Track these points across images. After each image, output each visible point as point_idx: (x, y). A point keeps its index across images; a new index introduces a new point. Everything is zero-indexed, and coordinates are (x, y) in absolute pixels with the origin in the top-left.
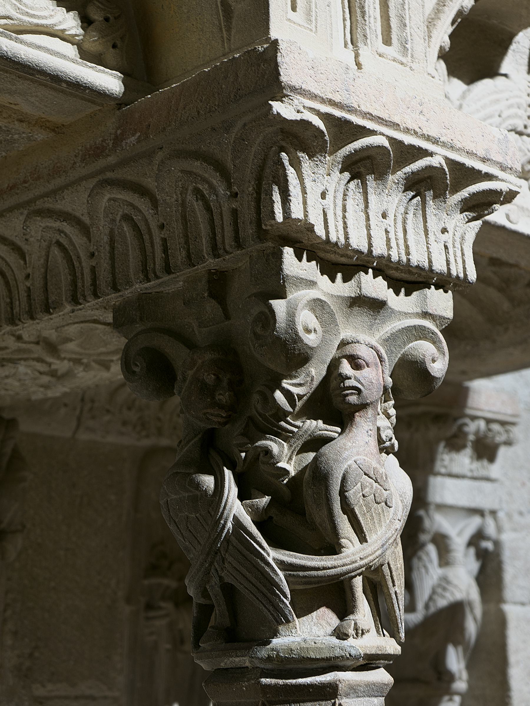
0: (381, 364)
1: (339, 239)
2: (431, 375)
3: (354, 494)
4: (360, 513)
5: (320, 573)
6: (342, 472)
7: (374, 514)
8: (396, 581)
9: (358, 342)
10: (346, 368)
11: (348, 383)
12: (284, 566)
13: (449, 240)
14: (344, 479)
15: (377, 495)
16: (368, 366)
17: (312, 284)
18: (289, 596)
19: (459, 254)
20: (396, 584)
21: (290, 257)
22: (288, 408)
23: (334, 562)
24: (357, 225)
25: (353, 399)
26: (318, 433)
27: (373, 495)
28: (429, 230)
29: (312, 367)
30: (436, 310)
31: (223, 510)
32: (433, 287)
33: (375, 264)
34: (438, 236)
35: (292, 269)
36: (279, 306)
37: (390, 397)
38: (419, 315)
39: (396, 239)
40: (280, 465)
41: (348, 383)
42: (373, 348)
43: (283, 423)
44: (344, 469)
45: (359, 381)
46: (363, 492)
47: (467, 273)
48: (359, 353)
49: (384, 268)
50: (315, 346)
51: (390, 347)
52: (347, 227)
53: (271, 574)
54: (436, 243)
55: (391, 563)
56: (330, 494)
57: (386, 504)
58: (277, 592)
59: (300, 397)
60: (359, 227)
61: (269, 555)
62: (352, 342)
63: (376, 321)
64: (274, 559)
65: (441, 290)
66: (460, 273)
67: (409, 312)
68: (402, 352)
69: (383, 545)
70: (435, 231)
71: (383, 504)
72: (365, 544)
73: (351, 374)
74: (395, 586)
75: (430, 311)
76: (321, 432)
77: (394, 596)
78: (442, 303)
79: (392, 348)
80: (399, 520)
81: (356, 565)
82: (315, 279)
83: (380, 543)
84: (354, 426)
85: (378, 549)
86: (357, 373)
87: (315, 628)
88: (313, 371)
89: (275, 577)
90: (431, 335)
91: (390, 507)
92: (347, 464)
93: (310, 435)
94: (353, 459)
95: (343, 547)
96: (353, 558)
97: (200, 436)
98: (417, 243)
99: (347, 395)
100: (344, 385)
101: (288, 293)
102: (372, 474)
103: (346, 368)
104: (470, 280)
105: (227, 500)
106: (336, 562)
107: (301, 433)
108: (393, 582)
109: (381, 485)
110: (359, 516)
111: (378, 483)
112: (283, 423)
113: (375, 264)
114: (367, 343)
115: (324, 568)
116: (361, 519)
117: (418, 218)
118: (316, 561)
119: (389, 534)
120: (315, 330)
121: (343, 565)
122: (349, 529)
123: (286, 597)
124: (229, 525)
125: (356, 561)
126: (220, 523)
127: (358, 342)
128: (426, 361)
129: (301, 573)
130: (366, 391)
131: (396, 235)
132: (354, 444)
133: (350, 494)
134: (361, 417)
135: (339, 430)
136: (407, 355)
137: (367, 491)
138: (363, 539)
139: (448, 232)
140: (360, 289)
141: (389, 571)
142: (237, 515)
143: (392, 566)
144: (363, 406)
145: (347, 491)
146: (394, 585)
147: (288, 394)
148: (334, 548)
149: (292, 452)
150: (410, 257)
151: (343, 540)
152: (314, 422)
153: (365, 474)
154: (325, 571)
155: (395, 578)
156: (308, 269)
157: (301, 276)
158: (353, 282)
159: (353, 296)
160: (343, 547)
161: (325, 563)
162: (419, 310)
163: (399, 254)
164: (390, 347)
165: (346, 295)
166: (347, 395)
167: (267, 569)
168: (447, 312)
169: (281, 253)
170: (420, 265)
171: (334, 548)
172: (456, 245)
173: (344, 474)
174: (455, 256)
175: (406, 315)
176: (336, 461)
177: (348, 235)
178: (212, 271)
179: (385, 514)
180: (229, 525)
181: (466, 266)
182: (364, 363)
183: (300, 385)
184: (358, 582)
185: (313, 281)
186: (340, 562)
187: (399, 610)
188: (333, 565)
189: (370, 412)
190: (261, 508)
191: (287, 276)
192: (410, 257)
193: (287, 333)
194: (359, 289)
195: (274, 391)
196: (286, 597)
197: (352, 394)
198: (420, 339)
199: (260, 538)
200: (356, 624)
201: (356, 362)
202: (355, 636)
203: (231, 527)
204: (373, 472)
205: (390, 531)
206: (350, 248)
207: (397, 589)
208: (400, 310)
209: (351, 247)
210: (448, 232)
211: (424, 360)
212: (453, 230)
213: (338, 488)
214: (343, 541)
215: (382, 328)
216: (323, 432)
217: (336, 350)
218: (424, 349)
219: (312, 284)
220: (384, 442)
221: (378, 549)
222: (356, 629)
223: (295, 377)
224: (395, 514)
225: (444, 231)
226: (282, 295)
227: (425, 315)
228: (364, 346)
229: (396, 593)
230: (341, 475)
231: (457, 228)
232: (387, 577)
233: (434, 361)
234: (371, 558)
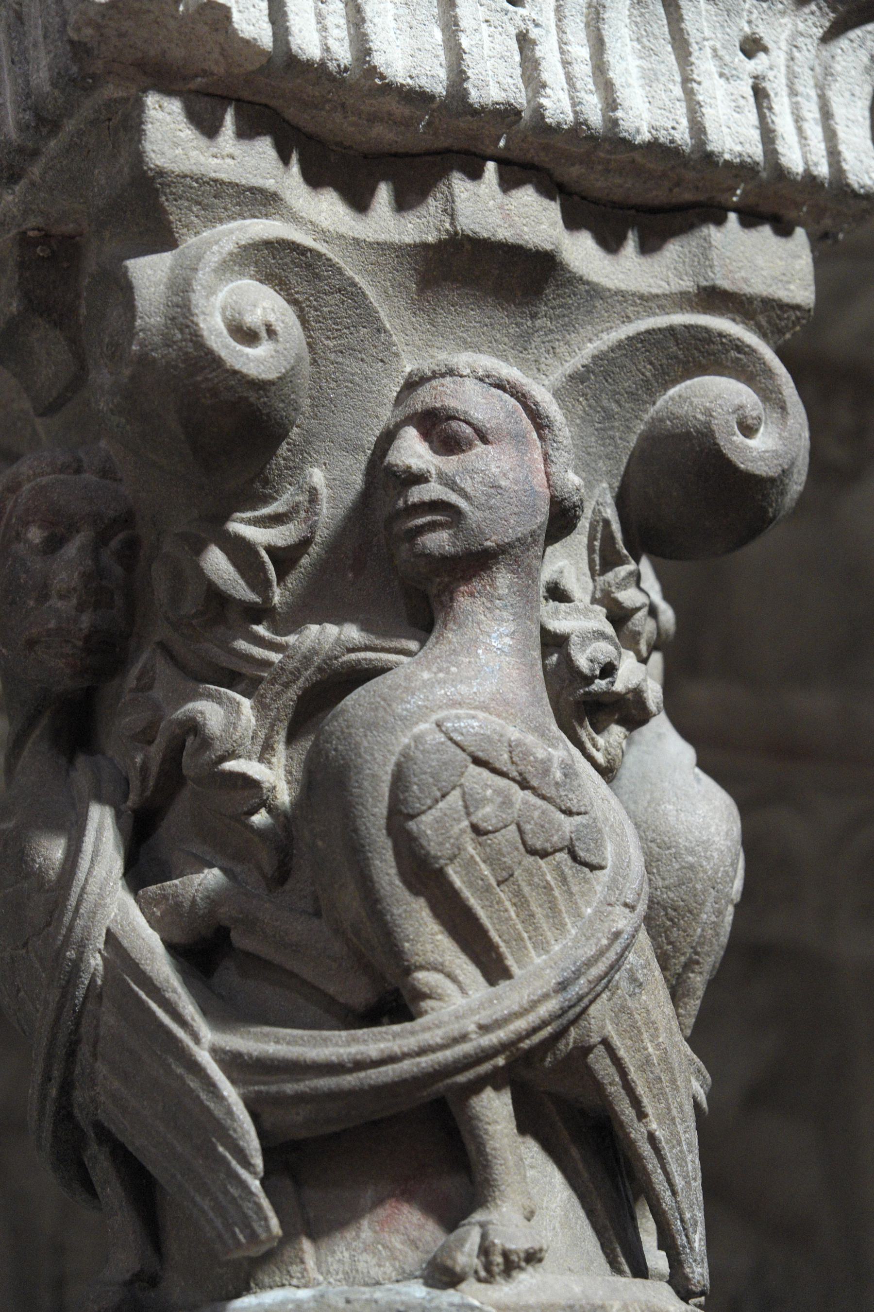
0: (541, 437)
1: (327, 50)
2: (736, 469)
3: (439, 826)
4: (471, 885)
5: (349, 1081)
6: (393, 759)
7: (526, 890)
8: (645, 1101)
9: (451, 372)
10: (413, 451)
11: (418, 494)
12: (236, 1065)
13: (770, 75)
14: (400, 779)
15: (527, 827)
16: (485, 440)
17: (263, 201)
18: (258, 1161)
19: (811, 111)
20: (649, 1110)
21: (168, 118)
22: (241, 590)
23: (389, 1044)
24: (409, 18)
25: (439, 541)
26: (345, 658)
27: (513, 827)
28: (692, 40)
29: (315, 463)
30: (746, 280)
31: (74, 919)
32: (732, 216)
33: (502, 144)
34: (727, 58)
35: (179, 151)
36: (150, 273)
37: (618, 552)
38: (690, 301)
39: (566, 63)
40: (230, 765)
41: (418, 494)
42: (504, 390)
43: (242, 645)
44: (398, 749)
45: (452, 485)
46: (474, 819)
47: (845, 166)
48: (452, 403)
49: (536, 154)
50: (272, 376)
51: (598, 400)
52: (363, 20)
53: (203, 1096)
54: (722, 81)
55: (616, 1041)
56: (356, 830)
57: (574, 857)
58: (221, 1149)
59: (286, 559)
60: (414, 23)
61: (197, 1040)
62: (435, 375)
63: (538, 323)
64: (216, 1052)
65: (766, 230)
66: (816, 164)
67: (655, 291)
68: (646, 417)
69: (563, 986)
70: (718, 46)
71: (563, 856)
72: (504, 985)
73: (423, 466)
74: (646, 1116)
75: (725, 284)
76: (353, 656)
77: (646, 1150)
78: (777, 265)
79: (605, 403)
80: (626, 905)
81: (465, 1048)
82: (270, 184)
83: (552, 978)
84: (451, 625)
85: (546, 997)
86: (450, 464)
87: (365, 1257)
88: (317, 476)
89: (212, 1106)
90: (733, 354)
91: (593, 868)
92: (409, 734)
93: (320, 669)
94: (435, 717)
95: (425, 996)
96: (454, 1029)
97: (44, 721)
98: (650, 78)
99: (421, 530)
100: (406, 502)
101: (179, 230)
102: (503, 760)
103: (413, 451)
104: (856, 186)
105: (83, 889)
106: (399, 1041)
107: (291, 665)
108: (636, 1103)
109: (544, 798)
110: (467, 894)
111: (534, 790)
112: (242, 645)
113: (502, 144)
114: (481, 373)
115: (360, 1065)
116: (474, 902)
117: (647, 7)
118: (337, 1045)
119: (590, 951)
120: (271, 332)
121: (422, 1051)
122: (439, 937)
123: (247, 1164)
124: (95, 961)
125: (463, 1038)
126: (64, 957)
127: (451, 372)
128: (715, 428)
129: (290, 1088)
130: (479, 514)
131: (562, 52)
132: (441, 675)
133: (425, 825)
134: (472, 595)
135: (413, 645)
136: (661, 420)
137: (486, 814)
138: (494, 969)
139: (765, 50)
140: (453, 216)
141: (612, 1070)
142: (116, 930)
143: (622, 1053)
144: (476, 562)
145: (412, 817)
146: (642, 1115)
147: (242, 553)
148: (396, 1002)
149: (272, 726)
150: (619, 114)
151: (422, 976)
152: (332, 630)
153: (478, 762)
154: (362, 1074)
155: (641, 1090)
156: (244, 159)
157: (213, 175)
158: (433, 205)
159: (431, 239)
160: (425, 996)
161: (362, 1048)
162: (687, 285)
163: (574, 105)
164: (598, 400)
165: (408, 240)
166: (421, 530)
167: (193, 1083)
168: (792, 287)
169: (140, 106)
170: (662, 140)
171: (396, 1002)
172: (800, 89)
173: (398, 765)
174: (798, 119)
175: (648, 302)
176: (371, 726)
177: (367, 41)
178: (31, 234)
179: (575, 889)
180: (95, 961)
181: (842, 148)
182: (469, 430)
183: (277, 520)
184: (495, 1110)
185: (261, 191)
186: (411, 1043)
187: (674, 1193)
188: (387, 1053)
189: (503, 579)
190: (187, 904)
191: (161, 173)
192: (619, 114)
193: (168, 342)
194: (448, 220)
195: (199, 549)
196: (247, 1164)
197: (433, 526)
198: (703, 371)
199: (175, 991)
200: (484, 1236)
201: (442, 430)
202: (483, 1274)
203: (101, 968)
204: (506, 756)
205: (593, 941)
206: (377, 81)
207: (654, 1126)
208: (623, 287)
209: (382, 77)
210: (765, 50)
211: (708, 425)
212: (784, 45)
213: (381, 809)
214: (424, 978)
215: (567, 343)
216: (362, 655)
217: (390, 406)
218: (713, 396)
219: (263, 201)
220: (589, 680)
221: (546, 997)
222: (485, 1250)
223: (266, 500)
224: (613, 885)
225: (752, 47)
226: (162, 238)
227: (713, 298)
228: (471, 386)
229: (652, 1138)
230: (390, 768)
231: (800, 41)
232: (611, 1089)
233: (748, 430)
234: (521, 1024)
